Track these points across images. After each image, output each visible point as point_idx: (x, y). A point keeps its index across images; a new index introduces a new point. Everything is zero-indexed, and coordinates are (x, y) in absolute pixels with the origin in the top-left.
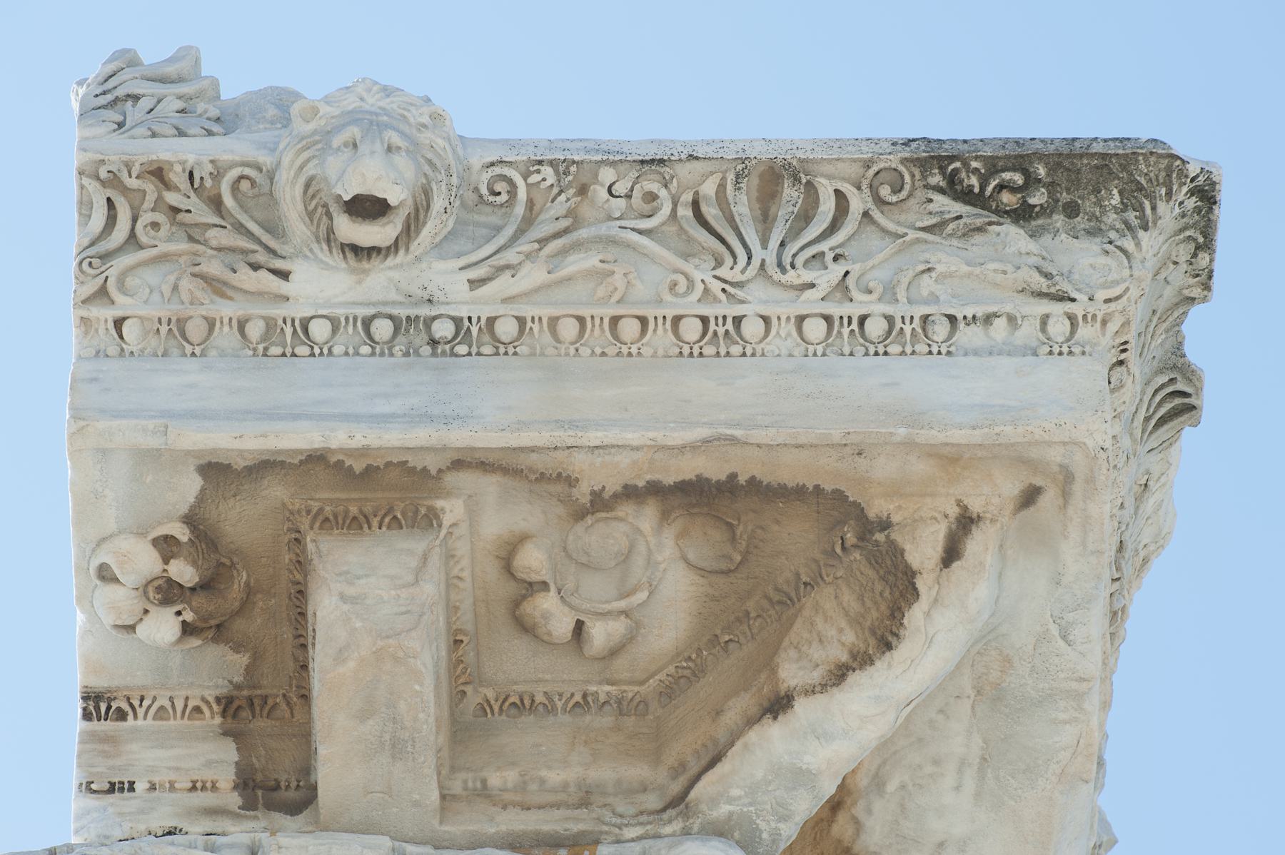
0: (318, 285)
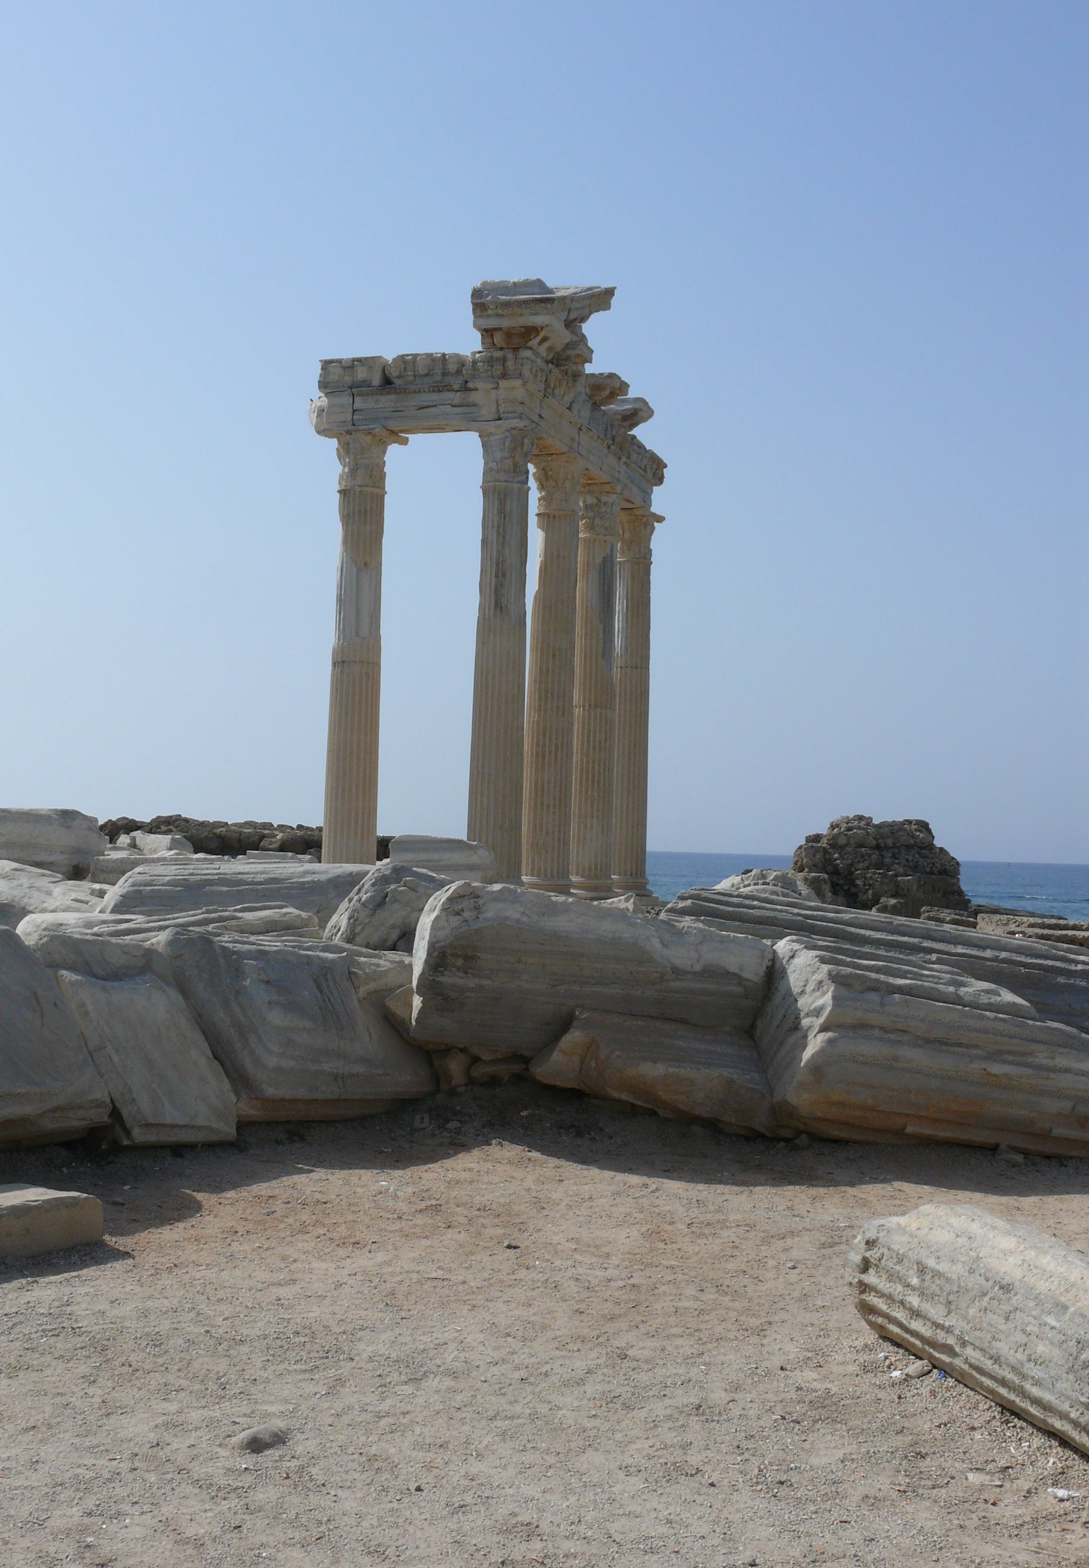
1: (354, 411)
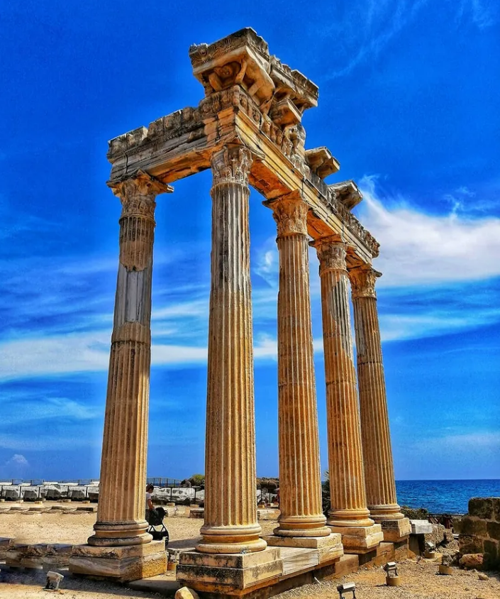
0: (203, 59)
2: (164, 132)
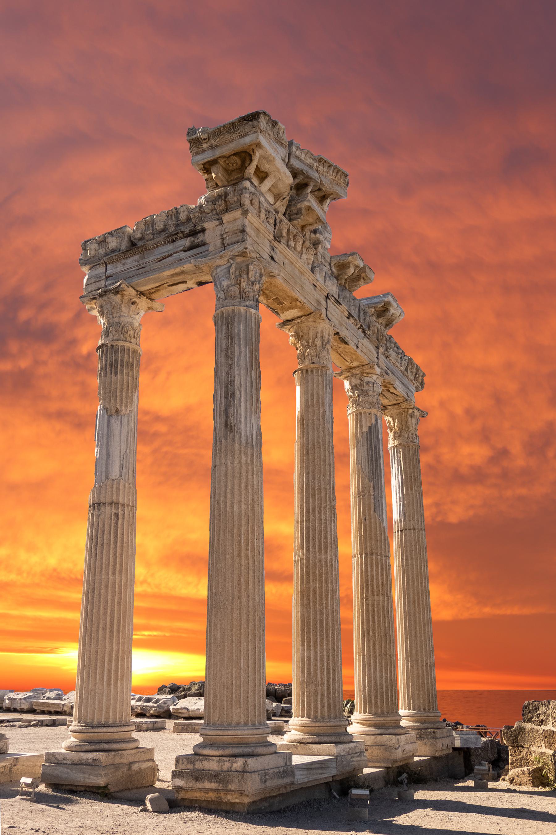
1: (107, 278)
2: (153, 234)
